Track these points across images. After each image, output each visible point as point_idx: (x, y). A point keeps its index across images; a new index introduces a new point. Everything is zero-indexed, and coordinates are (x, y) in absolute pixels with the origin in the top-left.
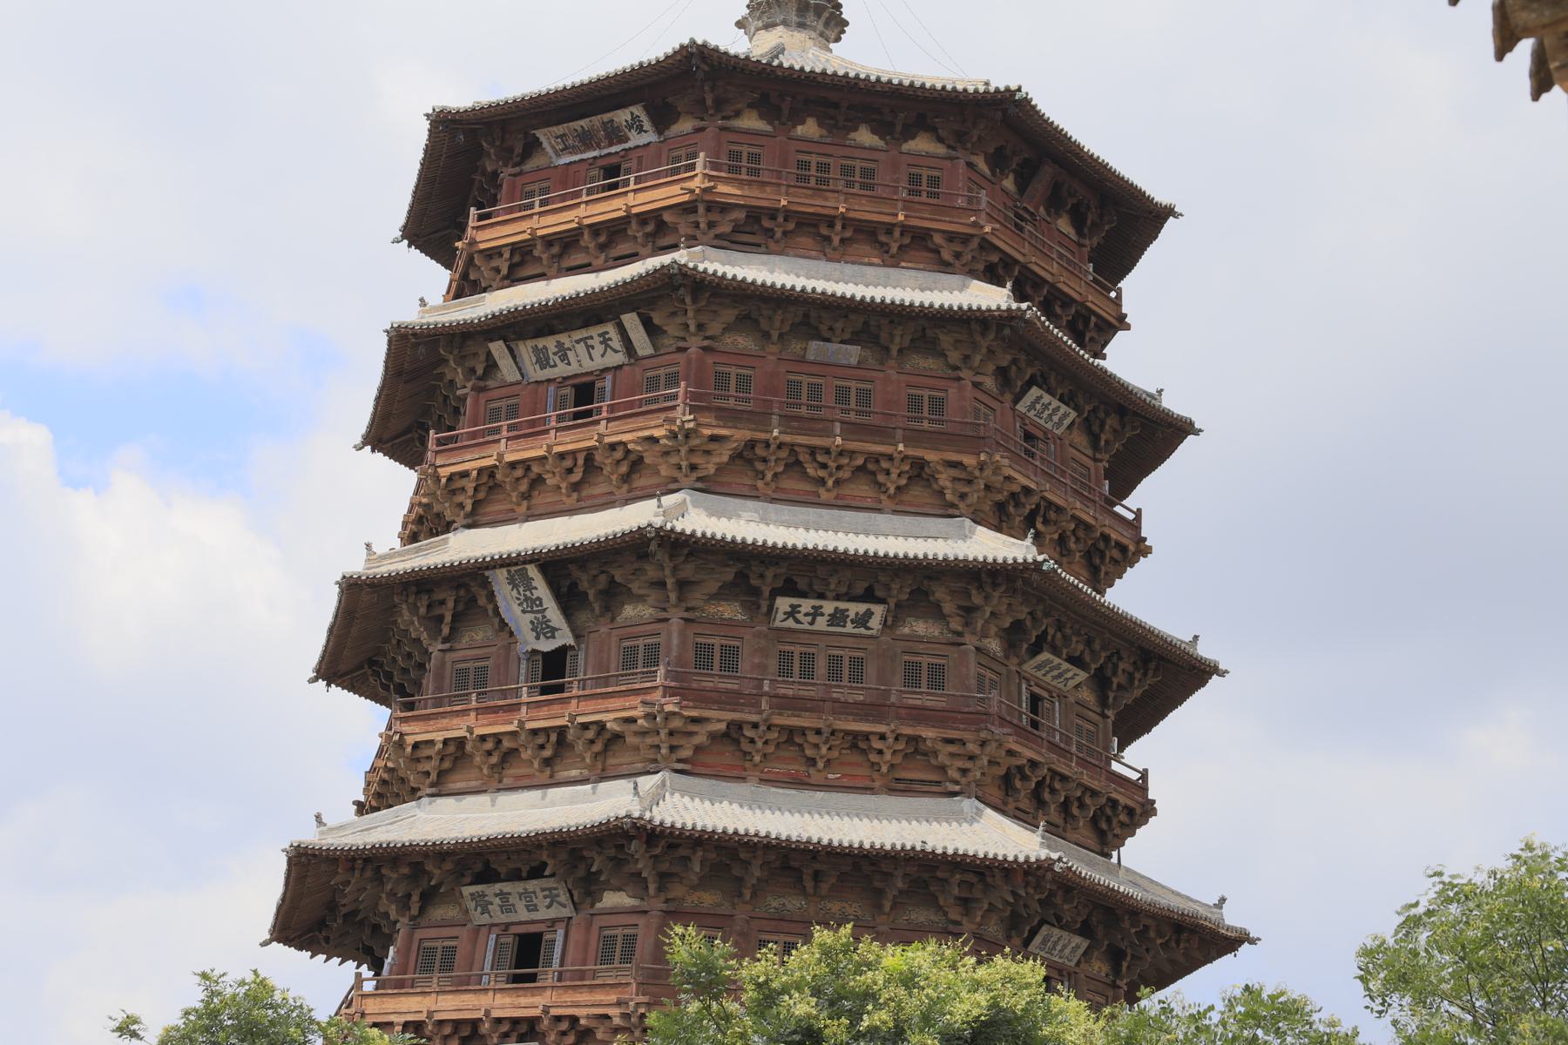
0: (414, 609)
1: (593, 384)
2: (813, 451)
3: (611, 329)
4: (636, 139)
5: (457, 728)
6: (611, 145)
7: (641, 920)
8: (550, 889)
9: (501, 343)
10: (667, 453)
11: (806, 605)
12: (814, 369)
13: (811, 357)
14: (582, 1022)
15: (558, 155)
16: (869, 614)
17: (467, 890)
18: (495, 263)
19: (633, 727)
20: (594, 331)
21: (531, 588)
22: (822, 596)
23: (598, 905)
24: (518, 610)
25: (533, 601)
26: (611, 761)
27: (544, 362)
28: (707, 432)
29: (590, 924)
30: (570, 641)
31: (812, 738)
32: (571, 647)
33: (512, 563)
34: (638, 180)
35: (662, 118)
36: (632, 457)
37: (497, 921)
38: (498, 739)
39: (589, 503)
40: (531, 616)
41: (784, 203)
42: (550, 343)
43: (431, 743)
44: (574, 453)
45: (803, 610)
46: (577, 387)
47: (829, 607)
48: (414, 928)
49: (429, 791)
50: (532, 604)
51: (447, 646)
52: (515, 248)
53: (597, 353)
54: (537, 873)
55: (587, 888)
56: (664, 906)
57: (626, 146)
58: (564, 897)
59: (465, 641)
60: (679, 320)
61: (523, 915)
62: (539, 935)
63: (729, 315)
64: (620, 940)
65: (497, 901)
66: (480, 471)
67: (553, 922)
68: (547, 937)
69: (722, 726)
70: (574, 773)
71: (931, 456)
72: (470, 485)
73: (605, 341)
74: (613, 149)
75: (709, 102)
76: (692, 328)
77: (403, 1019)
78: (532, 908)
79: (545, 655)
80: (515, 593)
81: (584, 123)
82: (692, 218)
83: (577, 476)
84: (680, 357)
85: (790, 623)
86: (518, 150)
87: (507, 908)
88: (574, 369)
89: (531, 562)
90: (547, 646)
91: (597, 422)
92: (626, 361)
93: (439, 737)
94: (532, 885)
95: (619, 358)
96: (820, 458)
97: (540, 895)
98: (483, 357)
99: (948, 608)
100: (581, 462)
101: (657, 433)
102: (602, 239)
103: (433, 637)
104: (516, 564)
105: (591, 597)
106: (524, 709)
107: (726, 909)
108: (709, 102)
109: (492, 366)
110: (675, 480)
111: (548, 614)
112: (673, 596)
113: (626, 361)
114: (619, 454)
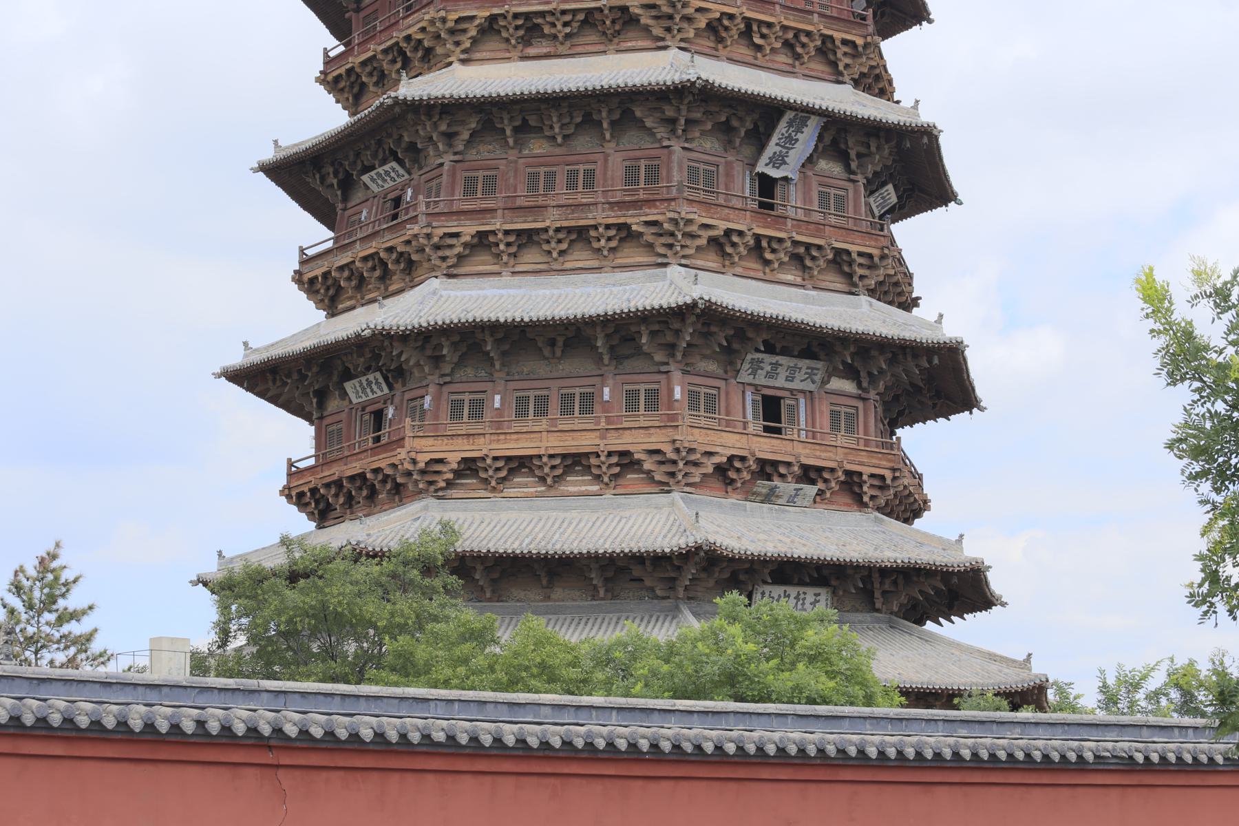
0: (689, 111)
7: (860, 405)
8: (812, 369)
10: (845, 54)
21: (799, 131)
26: (821, 277)
33: (806, 111)
37: (757, 382)
38: (758, 238)
39: (776, 66)
40: (778, 149)
44: (785, 28)
49: (683, 261)
50: (790, 141)
61: (780, 382)
62: (780, 398)
65: (769, 368)
70: (790, 278)
79: (763, 177)
87: (771, 375)
89: (825, 116)
90: (775, 173)
91: (811, 13)
93: (723, 225)
94: (804, 363)
97: (804, 371)
101: (860, 41)
104: (802, 111)
110: (841, 74)
111: (791, 153)
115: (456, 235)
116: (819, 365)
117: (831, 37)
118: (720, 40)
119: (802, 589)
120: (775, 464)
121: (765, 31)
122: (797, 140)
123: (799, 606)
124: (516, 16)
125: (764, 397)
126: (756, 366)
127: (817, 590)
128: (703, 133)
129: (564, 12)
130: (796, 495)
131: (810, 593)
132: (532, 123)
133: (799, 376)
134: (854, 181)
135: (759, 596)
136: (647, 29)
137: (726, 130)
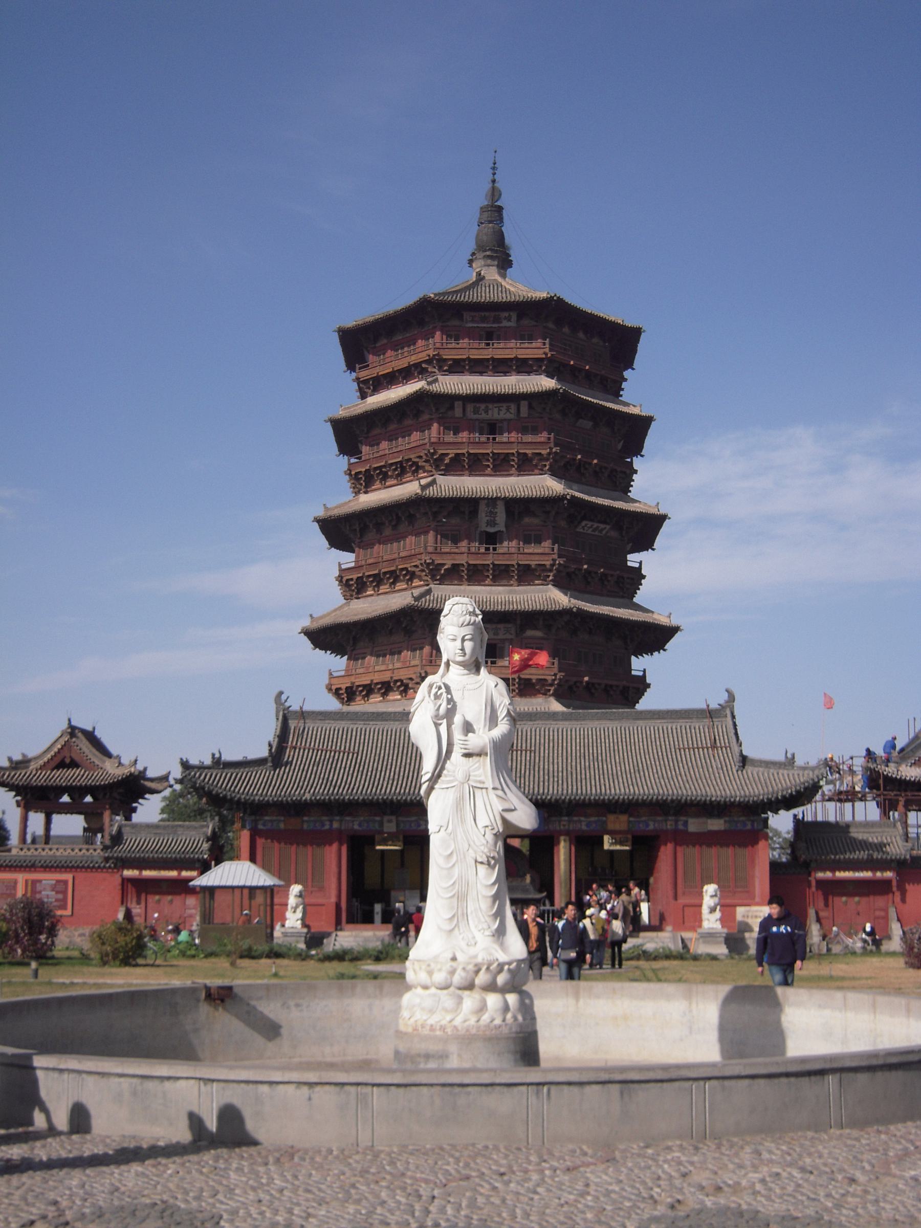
1: (495, 424)
3: (513, 407)
4: (505, 323)
5: (462, 560)
6: (494, 322)
9: (461, 403)
10: (541, 460)
11: (590, 524)
19: (543, 568)
20: (505, 405)
22: (592, 520)
24: (484, 515)
27: (476, 411)
30: (504, 529)
35: (519, 318)
38: (475, 565)
41: (572, 363)
42: (483, 406)
46: (489, 424)
47: (596, 525)
50: (492, 514)
53: (502, 413)
55: (522, 629)
57: (501, 325)
58: (513, 631)
68: (499, 645)
71: (619, 469)
72: (447, 461)
73: (508, 409)
79: (487, 533)
81: (487, 314)
83: (497, 463)
88: (489, 416)
94: (501, 626)
95: (512, 416)
96: (587, 466)
100: (502, 457)
101: (544, 452)
106: (491, 555)
114: (521, 457)
115: (352, 579)
116: (510, 625)
124: (376, 469)
129: (392, 464)
136: (423, 467)
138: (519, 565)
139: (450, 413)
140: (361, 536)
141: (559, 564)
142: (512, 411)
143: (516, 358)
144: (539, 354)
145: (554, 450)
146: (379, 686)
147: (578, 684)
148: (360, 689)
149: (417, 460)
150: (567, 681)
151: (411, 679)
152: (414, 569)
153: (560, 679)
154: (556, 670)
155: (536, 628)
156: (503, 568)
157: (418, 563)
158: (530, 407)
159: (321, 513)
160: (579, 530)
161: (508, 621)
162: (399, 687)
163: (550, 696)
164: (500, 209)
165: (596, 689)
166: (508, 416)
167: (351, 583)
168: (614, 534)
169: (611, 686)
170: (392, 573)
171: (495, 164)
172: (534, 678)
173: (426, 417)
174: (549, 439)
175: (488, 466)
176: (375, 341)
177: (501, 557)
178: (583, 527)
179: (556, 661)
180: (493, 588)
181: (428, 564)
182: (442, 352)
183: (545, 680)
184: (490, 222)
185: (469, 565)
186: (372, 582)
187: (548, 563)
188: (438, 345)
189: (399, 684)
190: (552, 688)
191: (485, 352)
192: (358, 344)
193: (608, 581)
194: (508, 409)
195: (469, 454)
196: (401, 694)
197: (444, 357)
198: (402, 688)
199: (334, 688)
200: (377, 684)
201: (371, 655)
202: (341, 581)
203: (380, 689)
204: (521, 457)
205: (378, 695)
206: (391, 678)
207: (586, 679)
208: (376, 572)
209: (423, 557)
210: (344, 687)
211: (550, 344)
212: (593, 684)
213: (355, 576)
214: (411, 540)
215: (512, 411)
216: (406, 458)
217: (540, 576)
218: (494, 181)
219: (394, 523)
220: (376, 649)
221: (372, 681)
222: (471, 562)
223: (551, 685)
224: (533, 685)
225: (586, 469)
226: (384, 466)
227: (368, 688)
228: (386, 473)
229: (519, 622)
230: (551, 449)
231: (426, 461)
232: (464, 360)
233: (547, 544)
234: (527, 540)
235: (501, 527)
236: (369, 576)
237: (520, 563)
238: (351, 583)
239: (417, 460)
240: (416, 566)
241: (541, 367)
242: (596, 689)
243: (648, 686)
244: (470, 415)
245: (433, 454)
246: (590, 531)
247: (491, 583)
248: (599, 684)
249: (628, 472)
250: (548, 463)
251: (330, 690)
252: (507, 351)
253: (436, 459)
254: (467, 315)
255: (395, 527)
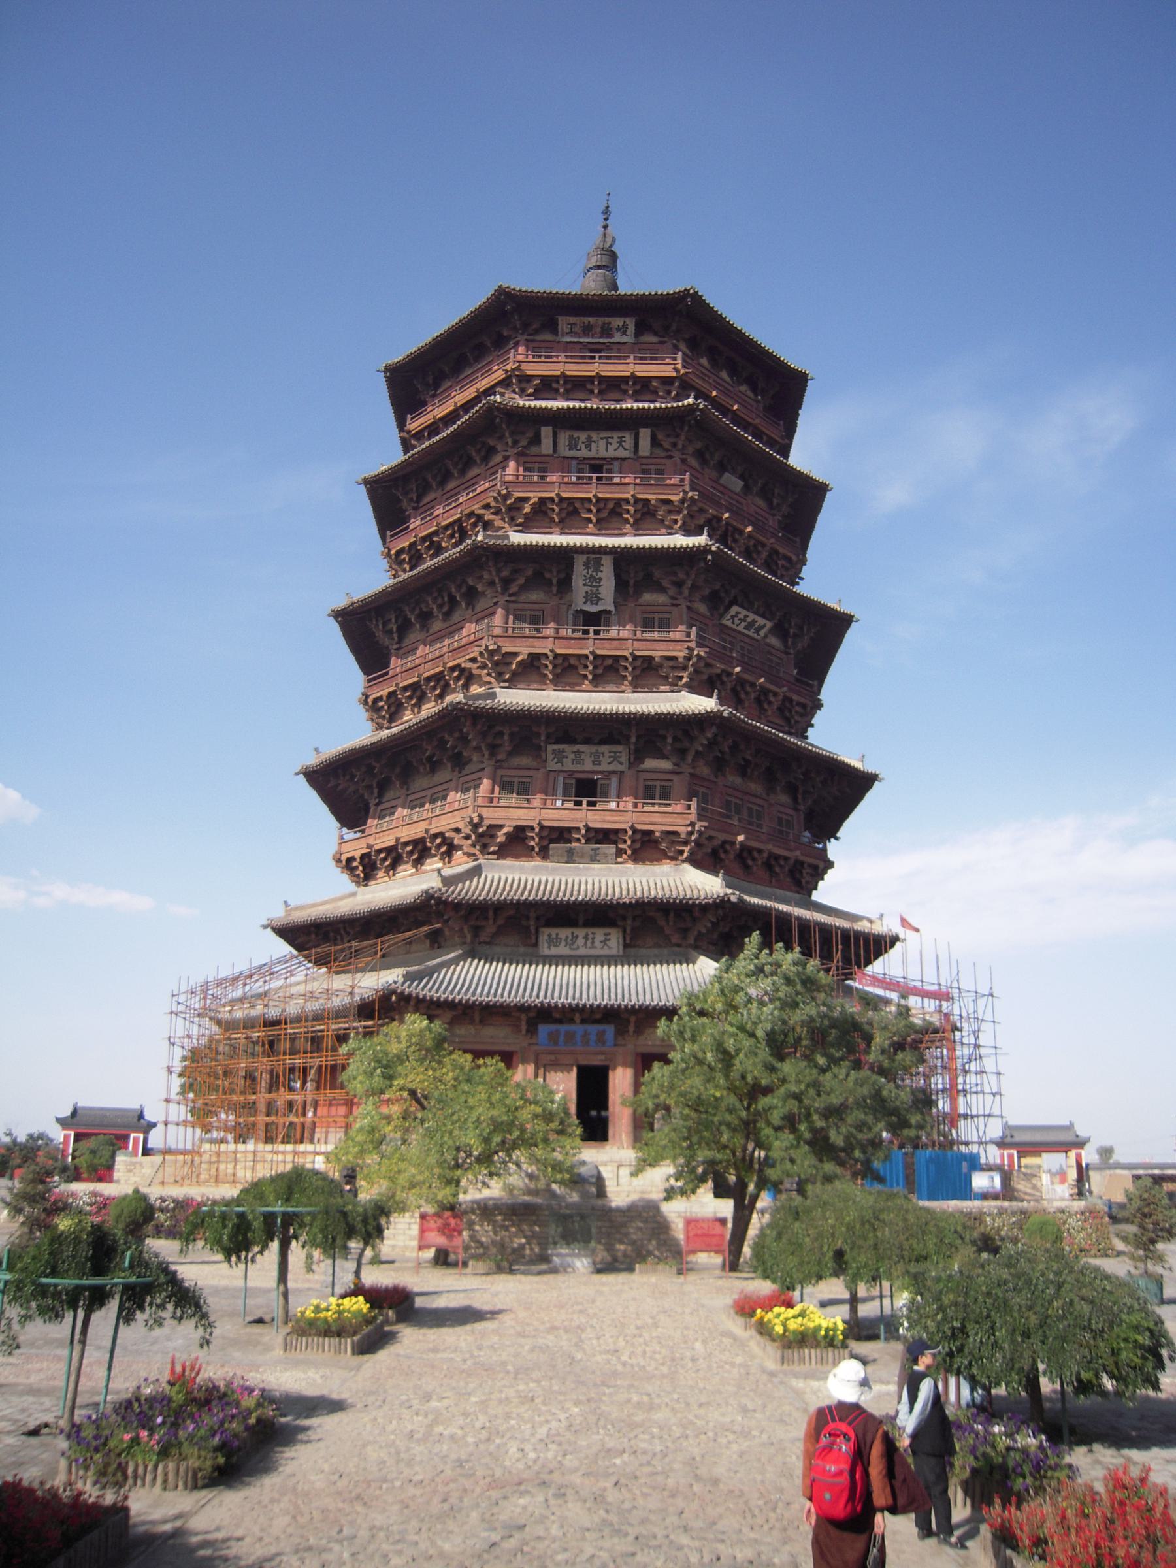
0: (499, 571)
2: (736, 529)
4: (618, 338)
5: (544, 647)
7: (675, 778)
9: (550, 428)
10: (670, 512)
11: (744, 612)
12: (721, 489)
13: (722, 481)
14: (657, 834)
15: (563, 335)
16: (764, 626)
17: (551, 748)
18: (524, 385)
19: (671, 663)
20: (616, 435)
21: (597, 570)
23: (642, 766)
24: (581, 583)
25: (595, 579)
27: (573, 446)
28: (700, 505)
29: (637, 779)
30: (612, 608)
31: (748, 689)
32: (610, 612)
34: (635, 358)
35: (641, 329)
36: (645, 510)
38: (566, 657)
40: (588, 589)
42: (583, 436)
43: (516, 654)
45: (741, 616)
47: (752, 617)
48: (496, 768)
50: (595, 581)
51: (513, 599)
52: (543, 378)
54: (609, 740)
55: (638, 757)
56: (692, 771)
58: (624, 758)
59: (522, 598)
60: (672, 440)
61: (588, 766)
62: (595, 782)
63: (699, 445)
64: (658, 788)
65: (573, 756)
66: (540, 498)
67: (610, 773)
68: (600, 782)
69: (719, 671)
71: (781, 550)
72: (527, 509)
73: (620, 443)
74: (602, 340)
75: (674, 328)
76: (680, 446)
77: (515, 823)
78: (597, 762)
80: (585, 572)
81: (591, 320)
82: (667, 388)
84: (667, 462)
85: (729, 623)
86: (535, 326)
87: (578, 759)
88: (593, 454)
92: (632, 456)
94: (604, 749)
95: (626, 454)
96: (737, 536)
98: (530, 434)
99: (792, 631)
100: (611, 505)
102: (603, 387)
103: (503, 594)
105: (632, 582)
106: (591, 641)
107: (712, 778)
108: (674, 328)
109: (536, 440)
112: (686, 592)
113: (632, 456)
114: (640, 506)
115: (380, 698)
116: (620, 748)
117: (647, 500)
118: (552, 520)
119: (590, 931)
120: (570, 830)
121: (587, 505)
122: (600, 579)
123: (589, 944)
124: (424, 539)
125: (580, 782)
126: (560, 756)
127: (607, 930)
128: (523, 588)
129: (446, 527)
130: (596, 855)
131: (599, 934)
132: (424, 610)
133: (605, 760)
134: (677, 605)
135: (546, 937)
137: (538, 580)
138: (635, 658)
139: (534, 450)
140: (400, 641)
141: (698, 655)
142: (626, 445)
143: (634, 377)
144: (666, 371)
145: (690, 494)
146: (409, 848)
147: (727, 847)
148: (382, 855)
149: (482, 511)
150: (710, 838)
151: (457, 830)
152: (469, 665)
153: (700, 833)
154: (694, 818)
155: (663, 757)
156: (609, 662)
157: (475, 654)
158: (655, 442)
159: (341, 603)
160: (726, 621)
161: (618, 743)
162: (439, 846)
163: (683, 861)
164: (613, 256)
165: (754, 859)
166: (622, 453)
167: (381, 704)
168: (774, 641)
169: (777, 858)
170: (438, 677)
171: (607, 207)
172: (657, 829)
173: (498, 458)
174: (682, 480)
175: (589, 520)
176: (437, 385)
177: (607, 644)
178: (733, 617)
179: (694, 803)
180: (593, 694)
181: (492, 653)
182: (524, 366)
183: (676, 833)
184: (599, 267)
185: (556, 656)
186: (410, 698)
187: (681, 655)
188: (520, 358)
189: (438, 841)
190: (687, 849)
191: (589, 367)
192: (411, 383)
193: (770, 703)
194: (621, 442)
195: (562, 499)
196: (442, 859)
197: (529, 373)
198: (443, 849)
199: (344, 858)
200: (406, 844)
201: (404, 807)
202: (365, 703)
203: (411, 853)
204: (640, 506)
205: (408, 866)
206: (427, 831)
207: (741, 838)
208: (416, 679)
209: (484, 642)
210: (357, 855)
211: (684, 360)
212: (750, 850)
213: (384, 693)
214: (470, 629)
215: (626, 445)
216: (467, 512)
217: (666, 677)
218: (605, 227)
219: (445, 609)
220: (410, 798)
221: (398, 839)
222: (559, 651)
223: (686, 843)
224: (656, 842)
225: (735, 541)
226: (435, 533)
227: (394, 855)
228: (439, 543)
229: (633, 739)
230: (686, 493)
231: (497, 512)
232: (556, 378)
233: (678, 633)
234: (648, 624)
235: (607, 603)
236: (405, 689)
237: (638, 653)
238: (381, 704)
239: (482, 511)
240: (473, 660)
241: (669, 393)
242: (754, 859)
243: (830, 865)
244: (564, 451)
245: (505, 497)
246: (741, 628)
247: (591, 688)
248: (760, 851)
249: (794, 558)
250: (679, 518)
251: (339, 861)
252: (620, 367)
253: (510, 508)
254: (563, 322)
255: (447, 615)
